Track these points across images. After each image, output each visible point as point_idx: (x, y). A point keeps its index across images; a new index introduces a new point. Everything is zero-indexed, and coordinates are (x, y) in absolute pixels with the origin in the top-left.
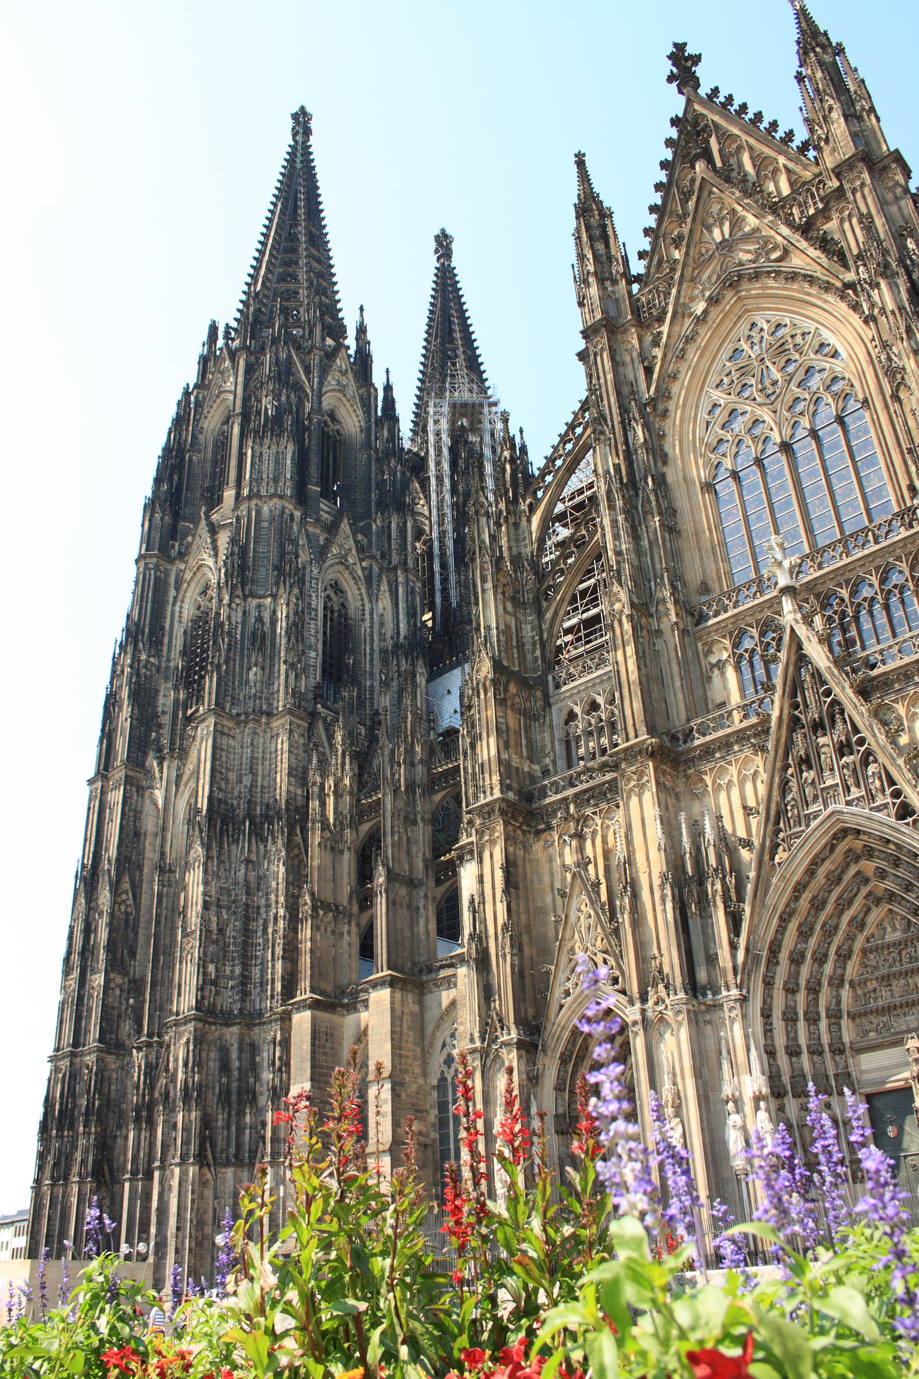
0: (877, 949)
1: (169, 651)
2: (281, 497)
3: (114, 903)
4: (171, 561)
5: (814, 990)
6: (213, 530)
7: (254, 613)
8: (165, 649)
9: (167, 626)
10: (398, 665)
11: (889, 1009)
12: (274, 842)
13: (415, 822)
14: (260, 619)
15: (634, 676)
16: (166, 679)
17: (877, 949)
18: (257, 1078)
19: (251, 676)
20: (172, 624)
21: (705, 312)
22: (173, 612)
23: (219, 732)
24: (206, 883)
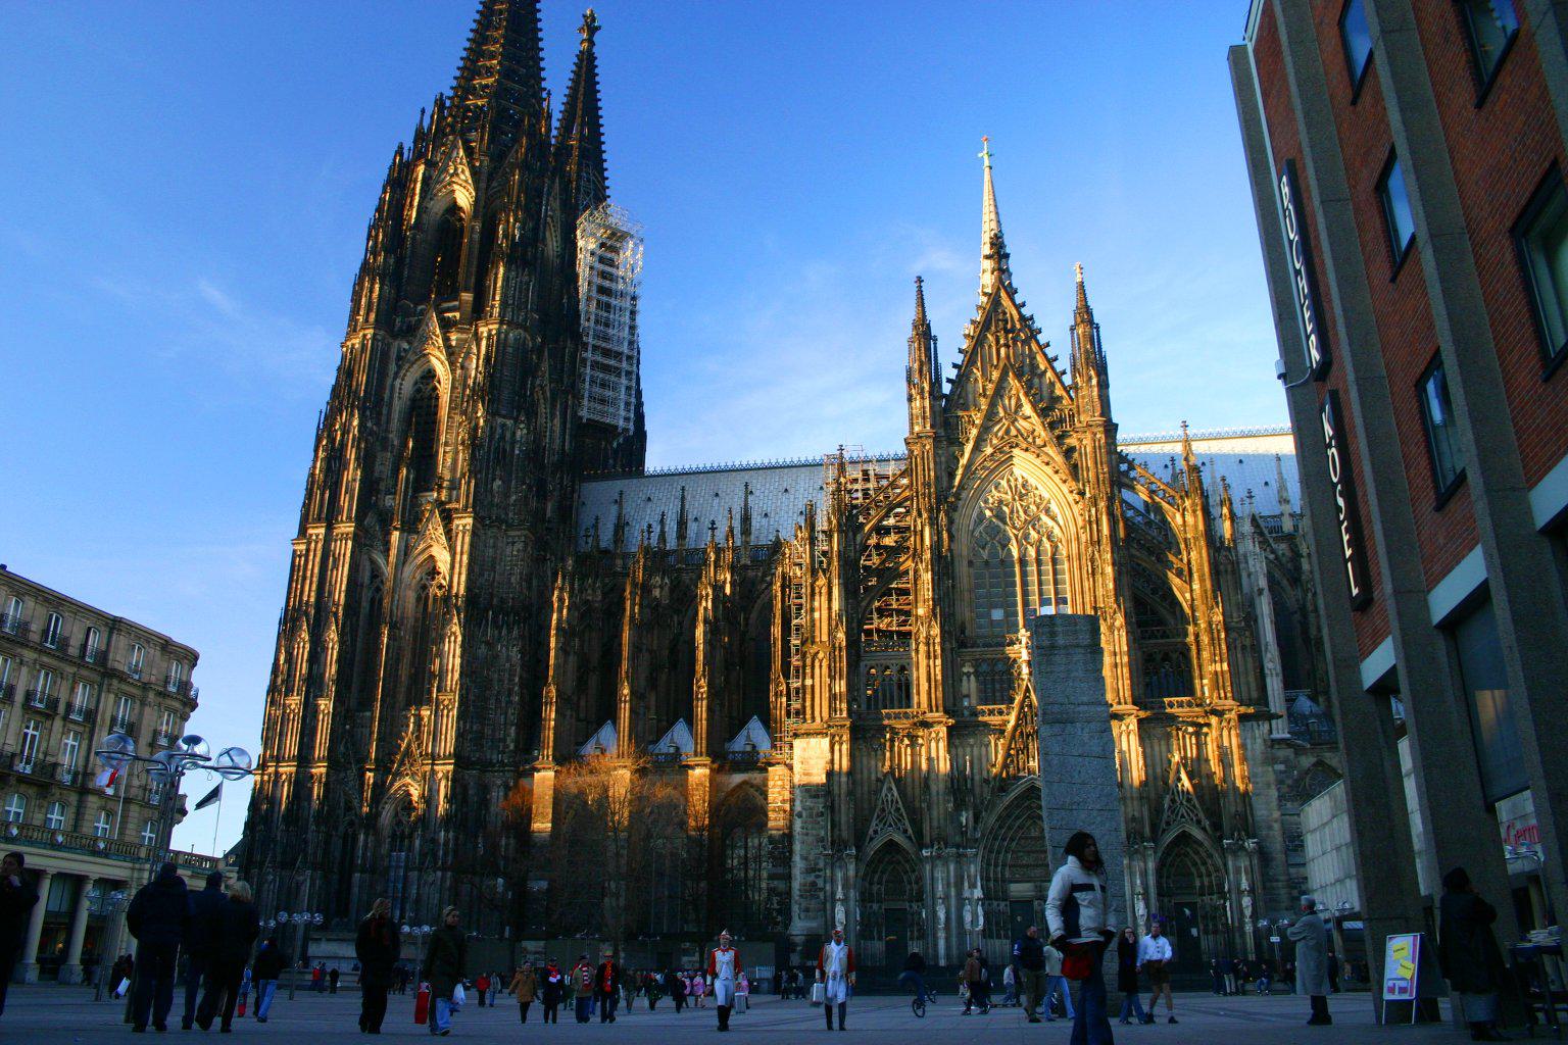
0: (1026, 838)
1: (388, 421)
2: (526, 329)
3: (342, 642)
4: (395, 337)
5: (999, 853)
6: (447, 326)
7: (499, 431)
8: (384, 418)
9: (386, 396)
10: (562, 478)
11: (1027, 866)
12: (510, 631)
13: (641, 650)
14: (502, 437)
15: (939, 677)
16: (385, 449)
17: (1026, 838)
18: (487, 808)
19: (495, 487)
20: (391, 397)
21: (992, 455)
22: (393, 386)
23: (474, 533)
24: (462, 657)
